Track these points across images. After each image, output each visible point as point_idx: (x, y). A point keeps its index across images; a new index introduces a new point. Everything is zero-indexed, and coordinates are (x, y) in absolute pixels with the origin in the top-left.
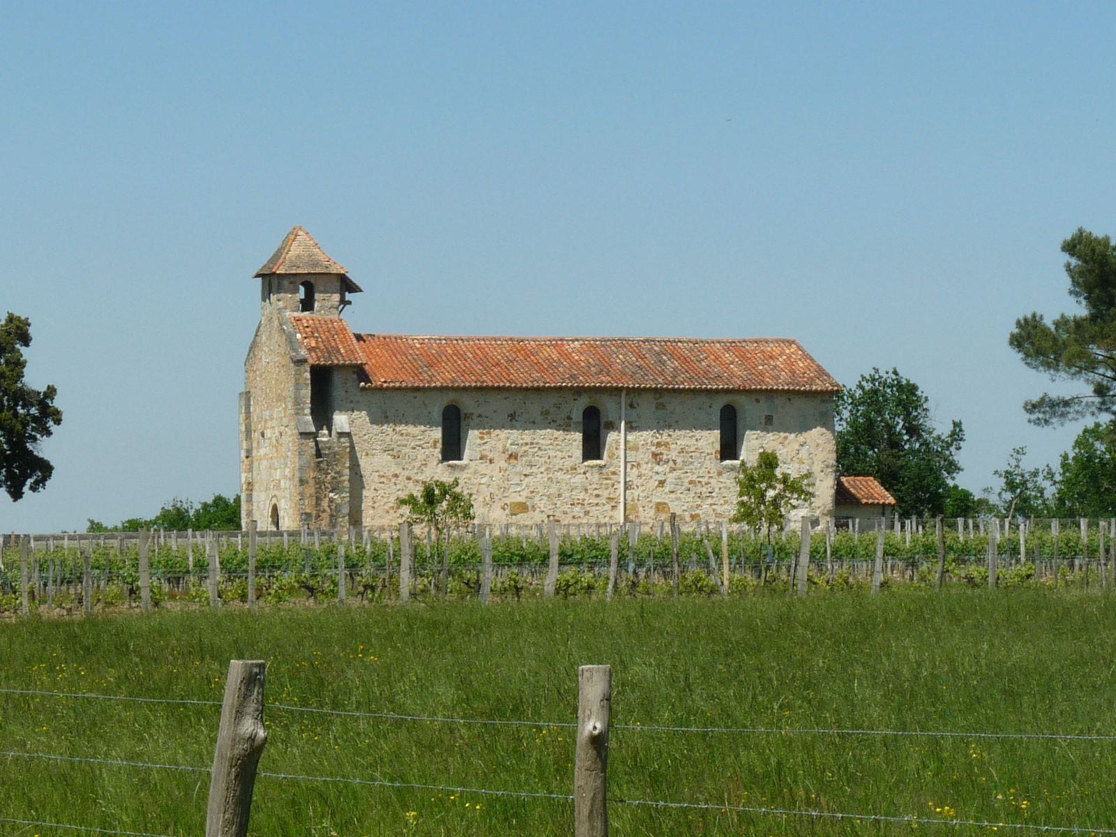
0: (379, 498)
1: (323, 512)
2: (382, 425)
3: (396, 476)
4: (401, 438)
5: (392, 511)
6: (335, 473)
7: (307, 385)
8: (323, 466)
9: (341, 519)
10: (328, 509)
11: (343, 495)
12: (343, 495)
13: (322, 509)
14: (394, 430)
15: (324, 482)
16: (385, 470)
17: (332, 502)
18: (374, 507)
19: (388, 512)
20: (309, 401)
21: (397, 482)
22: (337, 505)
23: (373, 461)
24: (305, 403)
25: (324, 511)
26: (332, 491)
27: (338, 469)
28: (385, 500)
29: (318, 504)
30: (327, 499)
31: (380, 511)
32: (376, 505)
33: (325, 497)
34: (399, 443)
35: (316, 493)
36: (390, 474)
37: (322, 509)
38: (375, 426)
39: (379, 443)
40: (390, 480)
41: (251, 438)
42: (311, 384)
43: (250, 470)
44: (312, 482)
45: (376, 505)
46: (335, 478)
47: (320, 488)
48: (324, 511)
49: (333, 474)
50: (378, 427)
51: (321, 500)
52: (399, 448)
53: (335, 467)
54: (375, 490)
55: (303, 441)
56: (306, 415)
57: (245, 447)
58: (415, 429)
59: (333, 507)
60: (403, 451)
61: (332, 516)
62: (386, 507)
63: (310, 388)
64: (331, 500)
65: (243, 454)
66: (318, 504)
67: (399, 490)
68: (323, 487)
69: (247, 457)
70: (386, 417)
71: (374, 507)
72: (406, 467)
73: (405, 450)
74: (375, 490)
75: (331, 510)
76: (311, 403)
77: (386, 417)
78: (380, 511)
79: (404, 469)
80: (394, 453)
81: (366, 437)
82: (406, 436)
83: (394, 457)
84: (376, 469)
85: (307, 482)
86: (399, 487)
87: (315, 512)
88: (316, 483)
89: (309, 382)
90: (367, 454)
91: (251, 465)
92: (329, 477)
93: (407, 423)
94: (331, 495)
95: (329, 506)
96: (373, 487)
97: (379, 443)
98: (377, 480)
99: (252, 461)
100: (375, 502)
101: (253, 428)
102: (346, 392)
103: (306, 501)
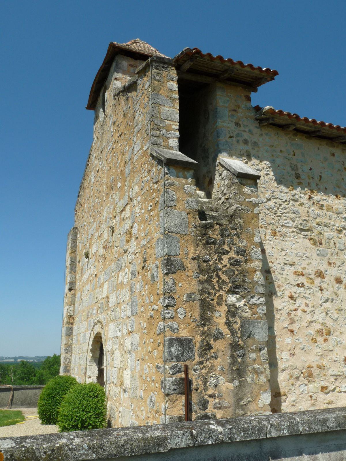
0: (299, 312)
1: (216, 338)
2: (294, 188)
3: (320, 274)
4: (321, 212)
5: (320, 339)
6: (237, 253)
7: (173, 100)
8: (214, 234)
9: (253, 355)
10: (226, 331)
11: (253, 301)
12: (253, 301)
13: (214, 330)
14: (310, 198)
15: (217, 270)
16: (304, 263)
17: (234, 315)
18: (292, 331)
19: (314, 341)
20: (176, 126)
21: (324, 286)
22: (245, 322)
23: (284, 245)
24: (168, 128)
25: (219, 336)
26: (232, 291)
27: (242, 245)
28: (309, 318)
29: (205, 320)
30: (224, 308)
31: (302, 339)
32: (295, 327)
33: (219, 304)
34: (318, 220)
35: (202, 292)
36: (310, 270)
37: (214, 330)
38: (282, 188)
39: (292, 216)
40: (313, 282)
41: (75, 272)
42: (180, 99)
43: (72, 303)
44: (191, 267)
45: (295, 327)
46: (236, 263)
47: (209, 281)
48: (219, 336)
49: (232, 254)
50: (287, 190)
51: (213, 310)
52: (319, 229)
53: (235, 240)
54: (291, 297)
55: (173, 179)
56: (172, 148)
57: (68, 279)
58: (337, 201)
59: (236, 327)
60: (326, 234)
61: (235, 347)
62: (312, 331)
63: (177, 106)
64: (233, 311)
65: (67, 287)
66: (205, 320)
67: (326, 301)
68: (215, 280)
69: (70, 290)
70: (298, 176)
71: (292, 331)
72: (332, 261)
73: (328, 233)
74: (291, 297)
75: (233, 333)
76: (180, 130)
77: (298, 176)
78: (302, 339)
79: (330, 264)
80: (314, 235)
81: (271, 203)
82: (328, 210)
83: (315, 243)
84: (290, 260)
85: (183, 268)
86: (327, 294)
87: (199, 338)
88: (201, 271)
89: (176, 96)
90: (274, 233)
91: (74, 298)
92: (225, 260)
93: (326, 191)
94: (232, 299)
95: (229, 324)
96: (287, 294)
97: (292, 216)
98: (292, 279)
99: (75, 294)
100: (292, 322)
101: (78, 260)
102: (237, 124)
103: (181, 310)
